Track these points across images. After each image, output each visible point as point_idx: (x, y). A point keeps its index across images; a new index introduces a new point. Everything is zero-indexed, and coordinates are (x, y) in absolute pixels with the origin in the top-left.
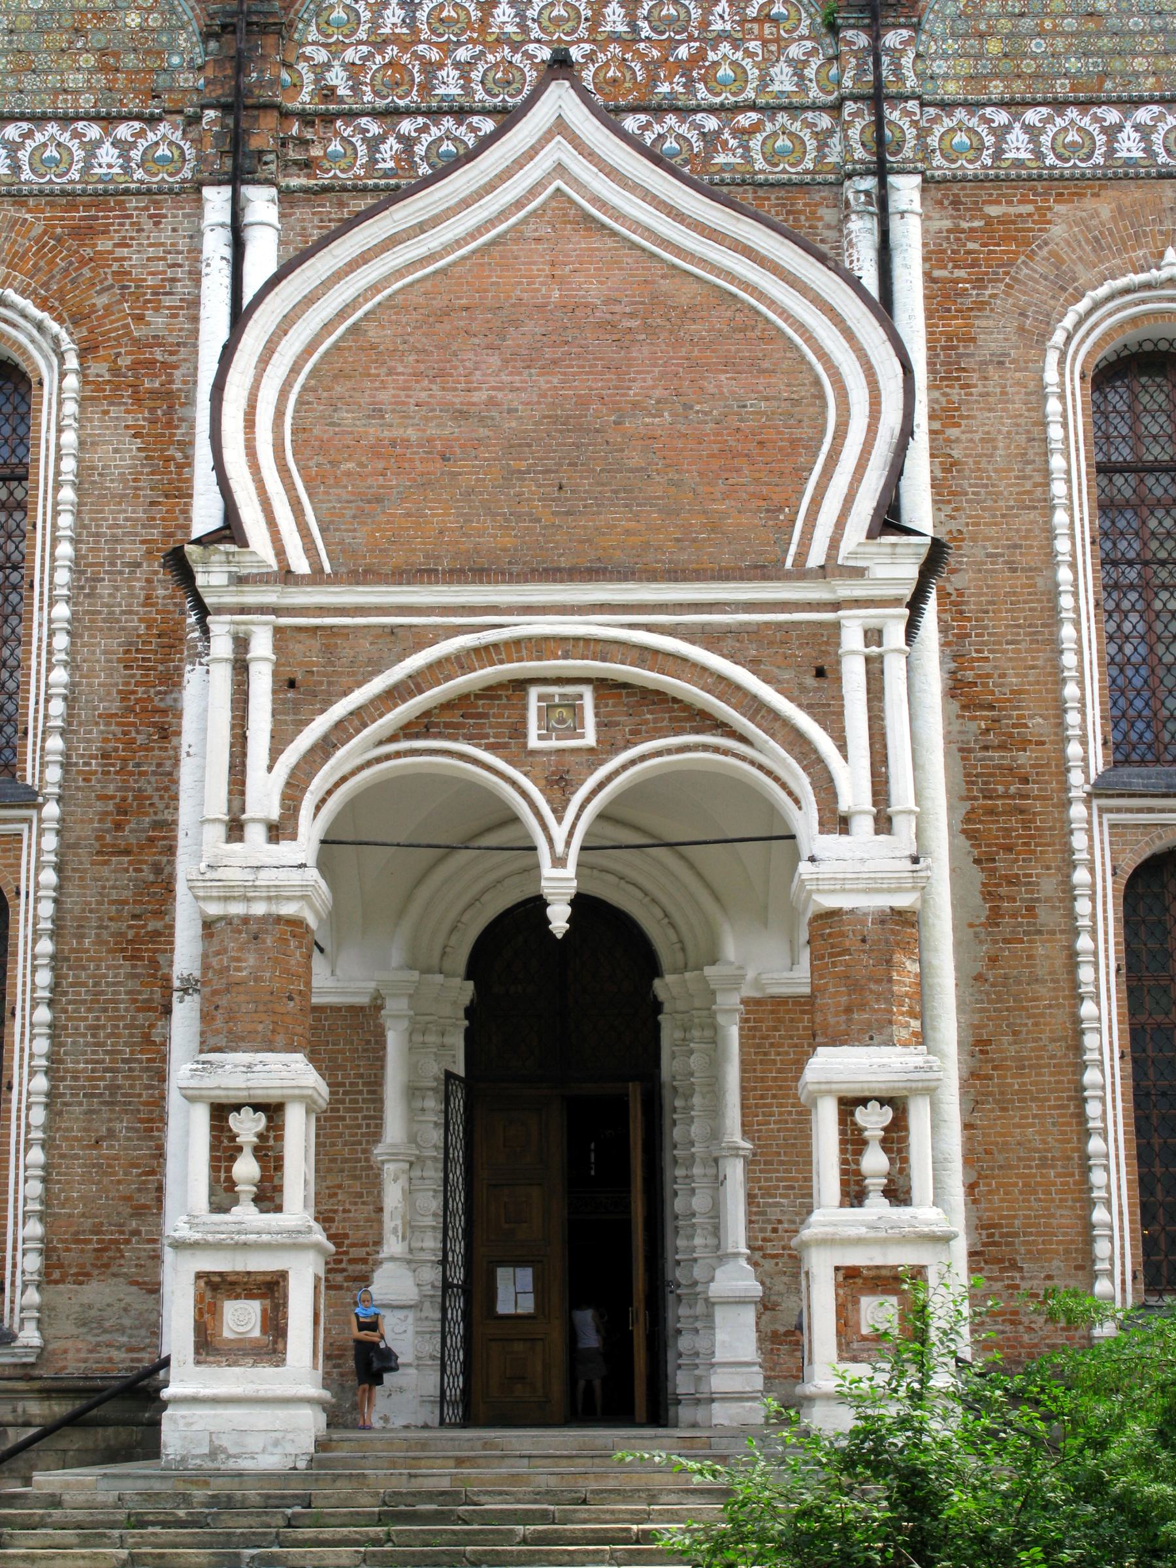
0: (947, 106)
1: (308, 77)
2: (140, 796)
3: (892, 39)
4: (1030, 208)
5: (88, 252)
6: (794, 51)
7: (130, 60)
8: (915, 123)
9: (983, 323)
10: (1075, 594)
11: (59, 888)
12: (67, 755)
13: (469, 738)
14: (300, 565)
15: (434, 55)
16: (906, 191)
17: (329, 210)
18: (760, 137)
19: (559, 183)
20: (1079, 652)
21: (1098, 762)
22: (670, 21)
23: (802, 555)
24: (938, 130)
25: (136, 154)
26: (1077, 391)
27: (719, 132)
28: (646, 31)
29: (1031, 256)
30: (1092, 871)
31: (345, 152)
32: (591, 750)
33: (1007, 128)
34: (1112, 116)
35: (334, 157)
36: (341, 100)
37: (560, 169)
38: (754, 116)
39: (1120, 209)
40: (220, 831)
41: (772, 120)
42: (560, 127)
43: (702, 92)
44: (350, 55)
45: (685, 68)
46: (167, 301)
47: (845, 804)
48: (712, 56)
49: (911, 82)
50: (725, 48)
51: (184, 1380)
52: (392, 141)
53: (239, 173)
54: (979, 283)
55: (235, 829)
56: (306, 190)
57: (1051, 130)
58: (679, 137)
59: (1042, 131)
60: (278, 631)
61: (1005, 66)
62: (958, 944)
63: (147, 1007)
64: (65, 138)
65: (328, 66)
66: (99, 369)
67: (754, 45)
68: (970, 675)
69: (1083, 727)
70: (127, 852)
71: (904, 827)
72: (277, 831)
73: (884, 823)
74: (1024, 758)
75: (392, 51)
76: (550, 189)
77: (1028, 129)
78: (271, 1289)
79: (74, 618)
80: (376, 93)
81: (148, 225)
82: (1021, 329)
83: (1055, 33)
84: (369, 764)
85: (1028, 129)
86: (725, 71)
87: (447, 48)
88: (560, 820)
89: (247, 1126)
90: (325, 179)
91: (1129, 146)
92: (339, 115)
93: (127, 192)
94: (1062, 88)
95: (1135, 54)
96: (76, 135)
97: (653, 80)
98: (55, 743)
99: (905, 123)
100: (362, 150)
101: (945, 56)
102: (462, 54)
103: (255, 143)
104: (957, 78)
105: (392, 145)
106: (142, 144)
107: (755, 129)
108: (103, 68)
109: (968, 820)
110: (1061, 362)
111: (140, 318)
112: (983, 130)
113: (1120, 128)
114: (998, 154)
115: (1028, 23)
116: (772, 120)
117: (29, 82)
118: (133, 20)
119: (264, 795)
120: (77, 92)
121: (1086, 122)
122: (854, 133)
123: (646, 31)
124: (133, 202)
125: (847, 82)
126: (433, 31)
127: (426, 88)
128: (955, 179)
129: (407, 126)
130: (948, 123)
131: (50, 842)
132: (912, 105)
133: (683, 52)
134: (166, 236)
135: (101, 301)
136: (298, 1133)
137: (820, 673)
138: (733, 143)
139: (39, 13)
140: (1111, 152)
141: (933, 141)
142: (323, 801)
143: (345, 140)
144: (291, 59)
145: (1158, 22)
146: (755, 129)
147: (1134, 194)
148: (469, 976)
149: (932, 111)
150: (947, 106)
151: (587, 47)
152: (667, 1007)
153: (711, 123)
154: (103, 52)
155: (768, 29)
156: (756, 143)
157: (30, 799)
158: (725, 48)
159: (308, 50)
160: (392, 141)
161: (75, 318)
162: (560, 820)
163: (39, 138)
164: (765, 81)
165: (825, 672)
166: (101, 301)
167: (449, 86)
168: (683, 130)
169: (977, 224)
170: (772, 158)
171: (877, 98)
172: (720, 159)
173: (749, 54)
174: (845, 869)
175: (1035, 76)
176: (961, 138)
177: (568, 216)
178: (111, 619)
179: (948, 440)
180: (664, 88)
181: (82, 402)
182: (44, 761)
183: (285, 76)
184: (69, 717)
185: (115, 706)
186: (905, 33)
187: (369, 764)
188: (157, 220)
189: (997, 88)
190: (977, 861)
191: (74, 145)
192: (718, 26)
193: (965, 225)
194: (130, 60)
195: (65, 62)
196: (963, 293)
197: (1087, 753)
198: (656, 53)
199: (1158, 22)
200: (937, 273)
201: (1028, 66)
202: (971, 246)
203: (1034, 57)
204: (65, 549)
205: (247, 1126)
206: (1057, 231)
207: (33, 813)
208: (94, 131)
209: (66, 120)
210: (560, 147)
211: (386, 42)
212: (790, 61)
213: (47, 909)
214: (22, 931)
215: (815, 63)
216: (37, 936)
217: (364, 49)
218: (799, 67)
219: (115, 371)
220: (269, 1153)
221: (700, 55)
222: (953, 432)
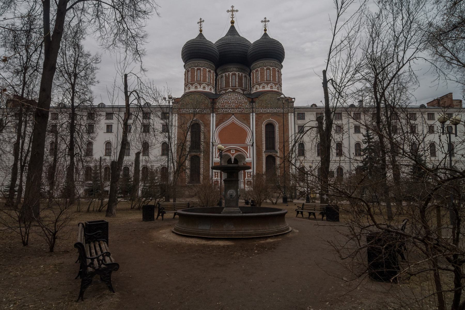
26: (264, 127)
31: (220, 111)
53: (213, 113)
89: (216, 173)
91: (268, 111)
165: (247, 149)
167: (226, 106)
171: (252, 108)
174: (248, 160)
177: (233, 123)
197: (264, 149)
205: (216, 173)
210: (233, 119)
220: (218, 174)
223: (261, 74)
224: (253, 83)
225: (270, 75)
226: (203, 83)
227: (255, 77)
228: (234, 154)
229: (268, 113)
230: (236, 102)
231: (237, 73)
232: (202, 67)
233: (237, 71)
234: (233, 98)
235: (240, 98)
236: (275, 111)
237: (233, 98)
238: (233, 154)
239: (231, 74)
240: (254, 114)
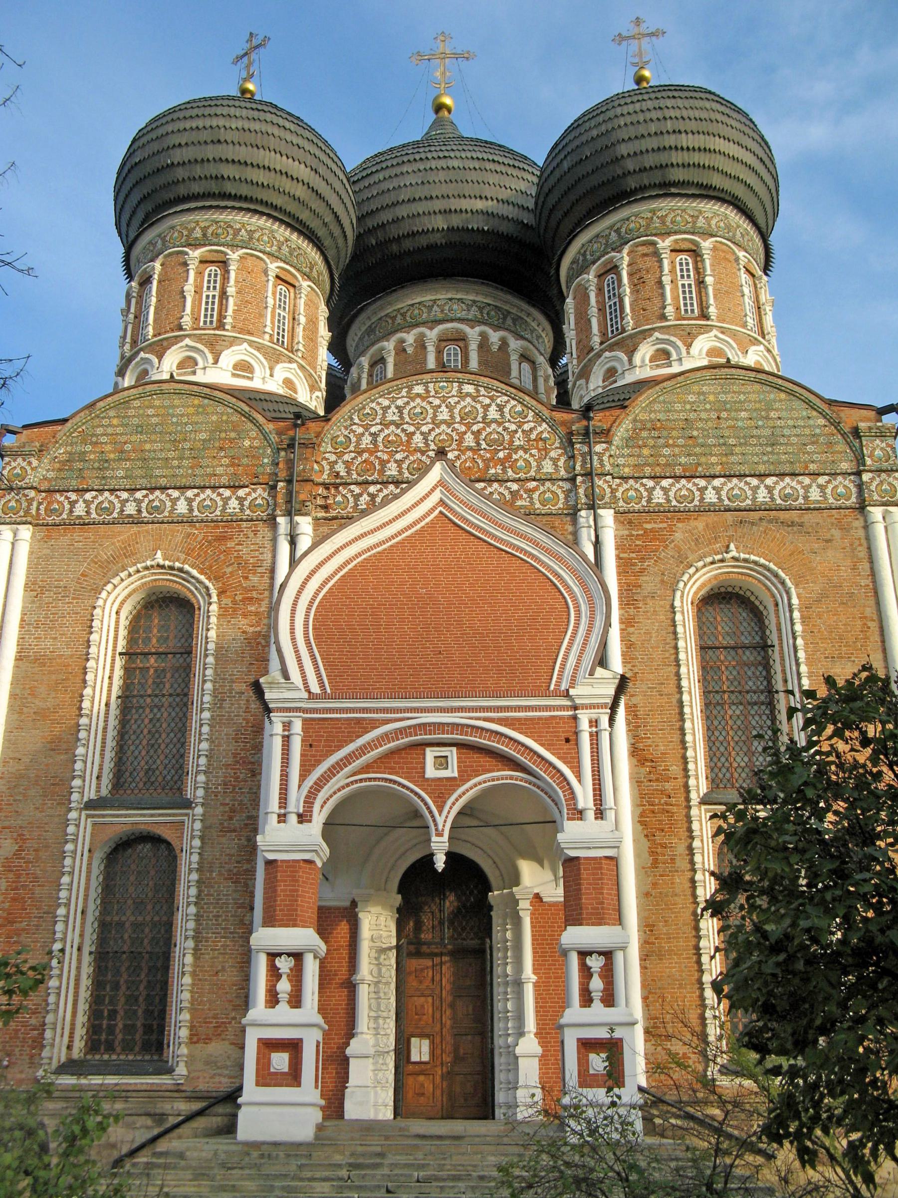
0: (625, 479)
1: (327, 467)
2: (241, 803)
3: (598, 448)
4: (665, 525)
5: (223, 548)
6: (553, 454)
7: (245, 461)
8: (610, 486)
9: (644, 578)
10: (691, 706)
11: (201, 848)
12: (206, 783)
13: (396, 774)
14: (315, 689)
15: (385, 457)
16: (607, 516)
17: (331, 522)
18: (537, 493)
19: (441, 508)
20: (694, 734)
21: (704, 788)
22: (495, 441)
23: (558, 684)
24: (621, 490)
25: (246, 503)
27: (518, 491)
28: (484, 446)
29: (666, 547)
30: (702, 841)
32: (454, 779)
33: (654, 488)
34: (702, 483)
35: (339, 503)
36: (342, 478)
37: (442, 502)
38: (534, 484)
39: (707, 525)
40: (274, 818)
41: (543, 485)
42: (441, 483)
43: (510, 473)
44: (346, 457)
45: (502, 462)
46: (259, 570)
47: (581, 805)
48: (514, 457)
49: (608, 468)
50: (521, 453)
51: (251, 1091)
52: (365, 496)
54: (643, 560)
55: (282, 818)
56: (325, 519)
57: (674, 489)
58: (500, 493)
59: (670, 490)
60: (305, 720)
61: (651, 460)
62: (637, 876)
63: (241, 906)
64: (214, 496)
65: (336, 462)
66: (227, 601)
67: (534, 452)
68: (641, 746)
69: (696, 770)
70: (235, 831)
71: (610, 815)
72: (303, 818)
73: (600, 814)
74: (668, 786)
75: (365, 456)
76: (437, 512)
77: (663, 488)
78: (294, 1047)
79: (212, 718)
80: (358, 475)
81: (251, 535)
82: (662, 581)
83: (674, 446)
84: (348, 785)
85: (663, 488)
86: (521, 463)
87: (392, 454)
88: (440, 813)
89: (284, 965)
90: (333, 513)
91: (711, 496)
92: (341, 484)
93: (241, 520)
94: (678, 471)
95: (711, 455)
96: (219, 494)
97: (487, 467)
98: (202, 778)
99: (605, 486)
100: (351, 500)
101: (623, 456)
102: (398, 456)
103: (302, 497)
104: (629, 466)
105: (365, 498)
106: (250, 498)
107: (533, 490)
108: (233, 465)
109: (641, 816)
110: (682, 596)
111: (246, 578)
112: (642, 489)
113: (706, 488)
114: (649, 500)
115: (662, 441)
116: (543, 485)
117: (197, 471)
118: (247, 443)
119: (296, 801)
120: (222, 475)
121: (690, 486)
122: (581, 491)
123: (484, 446)
124: (245, 524)
125: (578, 468)
126: (385, 447)
127: (382, 471)
128: (629, 512)
129: (372, 489)
130: (625, 486)
131: (198, 825)
132: (608, 478)
133: (501, 455)
134: (258, 540)
135: (229, 570)
136: (311, 968)
137: (567, 740)
138: (525, 496)
139: (204, 440)
140: (702, 499)
141: (619, 494)
142: (325, 803)
143: (343, 495)
144: (319, 460)
145: (721, 441)
146: (533, 490)
147: (712, 518)
148: (399, 892)
149: (618, 481)
150: (625, 479)
151: (456, 453)
152: (495, 909)
153: (515, 487)
154: (233, 458)
155: (541, 444)
156: (536, 496)
157: (188, 804)
158: (521, 453)
159: (327, 455)
160: (365, 496)
161: (216, 578)
162: (440, 813)
163: (202, 496)
164: (539, 467)
166: (229, 570)
167: (392, 470)
168: (502, 490)
169: (641, 532)
170: (543, 503)
172: (519, 503)
173: (532, 455)
175: (666, 465)
176: (632, 493)
178: (230, 719)
179: (629, 633)
180: (492, 471)
181: (219, 617)
182: (196, 787)
183: (316, 466)
184: (209, 765)
185: (230, 761)
186: (604, 446)
187: (348, 785)
188: (255, 533)
189: (648, 471)
190: (646, 836)
191: (218, 499)
192: (517, 443)
193: (634, 533)
194: (245, 461)
195: (215, 462)
196: (635, 565)
198: (488, 455)
199: (721, 441)
200: (622, 555)
201: (662, 461)
202: (638, 543)
203: (665, 456)
204: (209, 686)
206: (678, 536)
207: (190, 811)
208: (227, 493)
209: (214, 488)
211: (363, 451)
212: (551, 459)
213: (195, 858)
214: (183, 869)
215: (563, 459)
216: (190, 871)
217: (353, 455)
218: (555, 461)
219: (234, 602)
221: (510, 456)
222: (631, 630)
223: (638, 283)
224: (585, 349)
225: (701, 283)
226: (234, 341)
227: (593, 310)
228: (451, 784)
229: (705, 509)
230: (469, 440)
231: (473, 333)
232: (234, 247)
233: (472, 322)
234: (444, 415)
235: (493, 413)
236: (762, 495)
237: (444, 415)
238: (441, 790)
239: (432, 335)
240: (607, 516)
